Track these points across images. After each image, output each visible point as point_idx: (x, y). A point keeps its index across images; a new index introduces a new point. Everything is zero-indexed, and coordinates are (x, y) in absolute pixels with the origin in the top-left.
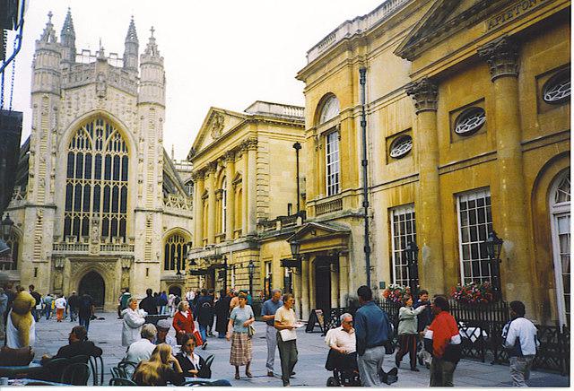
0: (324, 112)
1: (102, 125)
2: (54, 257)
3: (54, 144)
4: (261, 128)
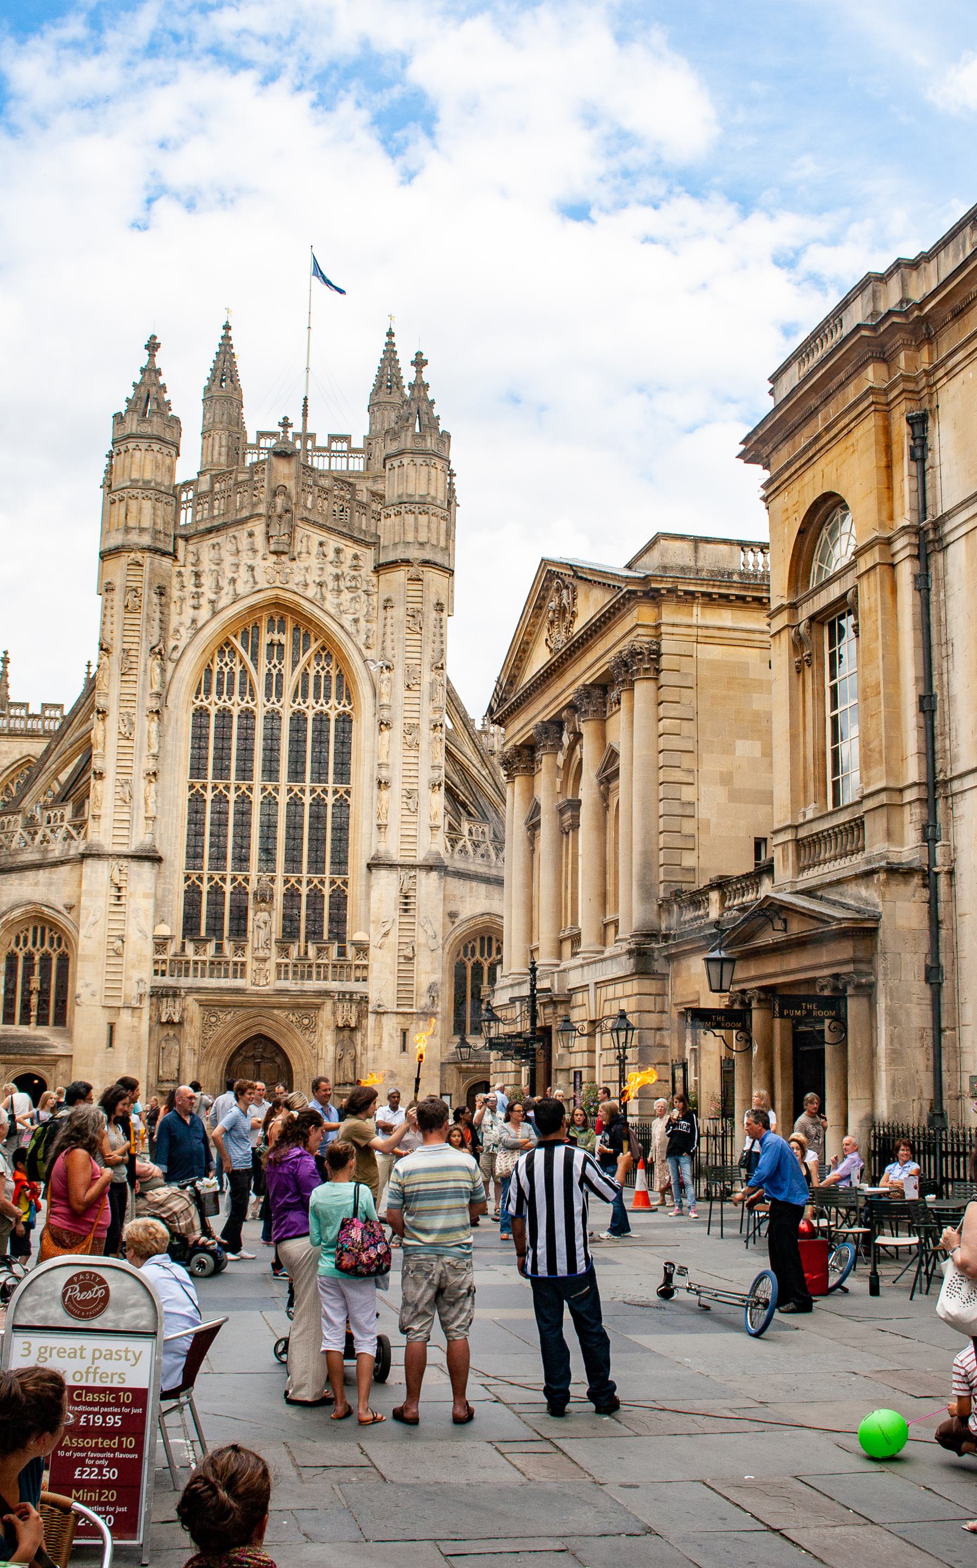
0: (817, 556)
1: (282, 630)
2: (159, 994)
3: (156, 688)
4: (670, 614)
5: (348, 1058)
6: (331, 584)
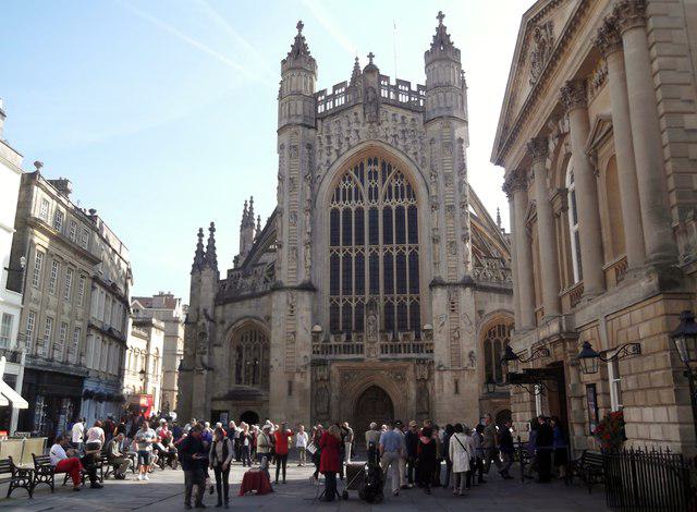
1: (376, 163)
2: (315, 364)
3: (308, 197)
5: (424, 398)
6: (400, 135)
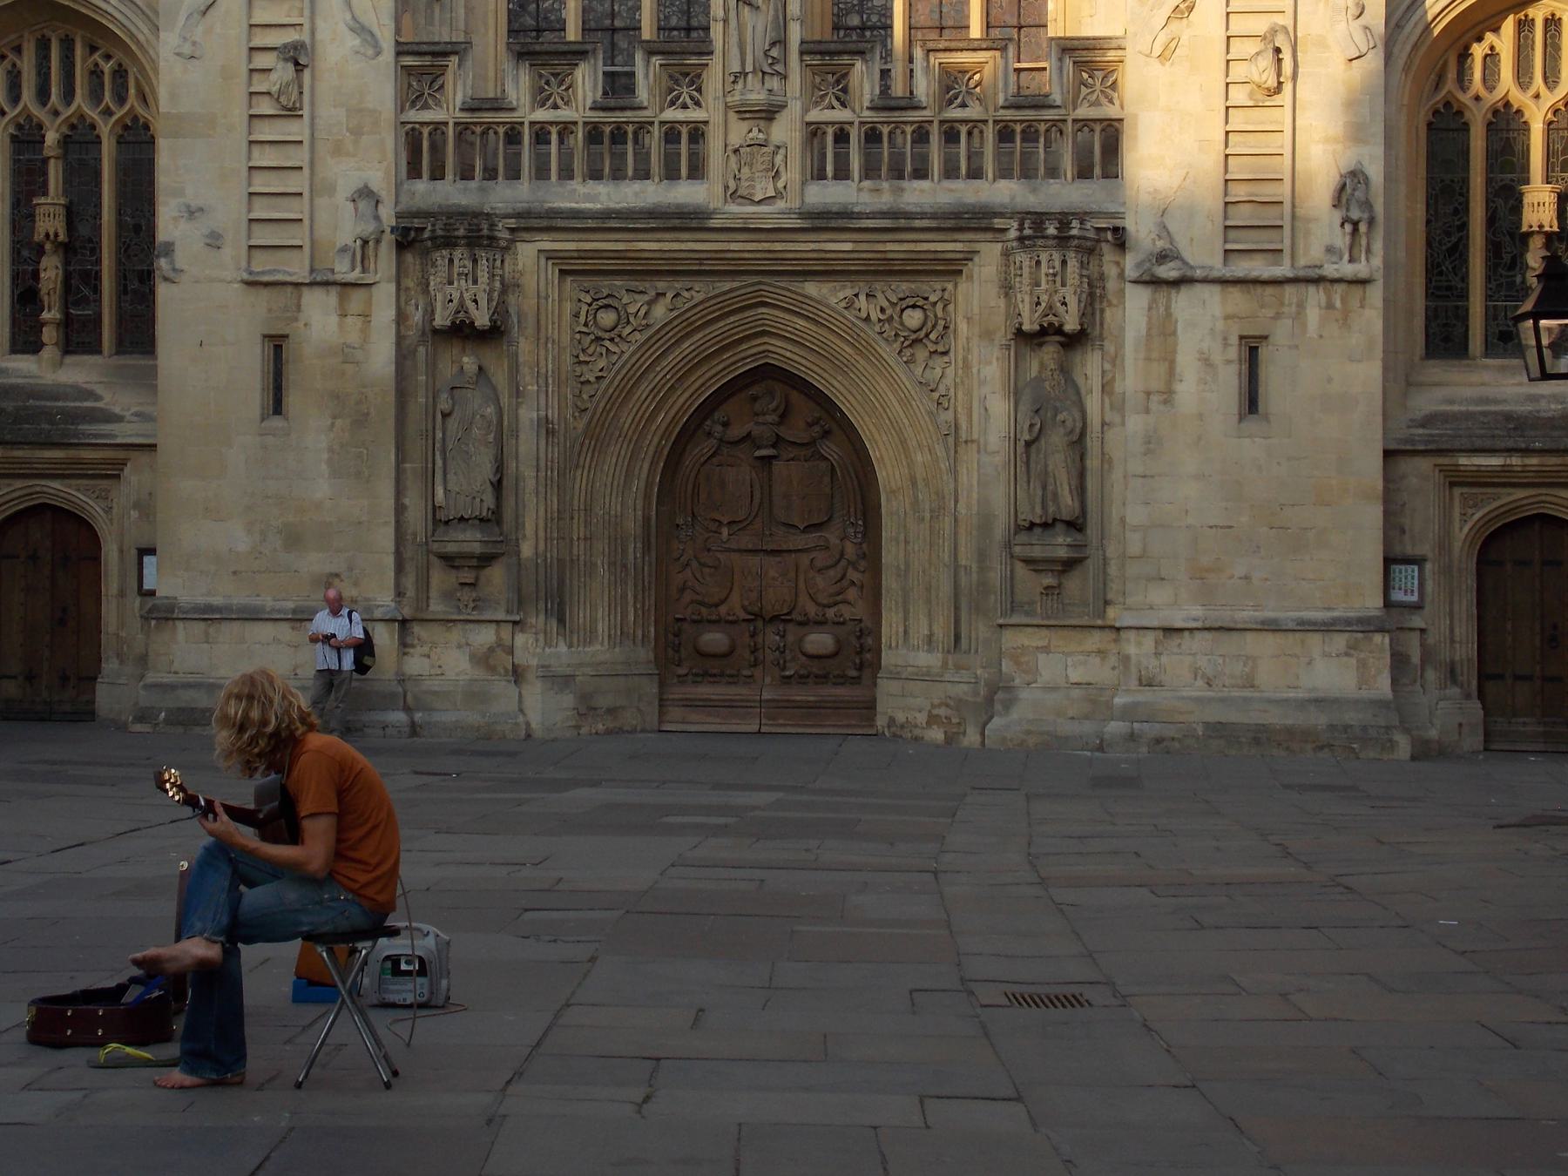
5: (1056, 440)
